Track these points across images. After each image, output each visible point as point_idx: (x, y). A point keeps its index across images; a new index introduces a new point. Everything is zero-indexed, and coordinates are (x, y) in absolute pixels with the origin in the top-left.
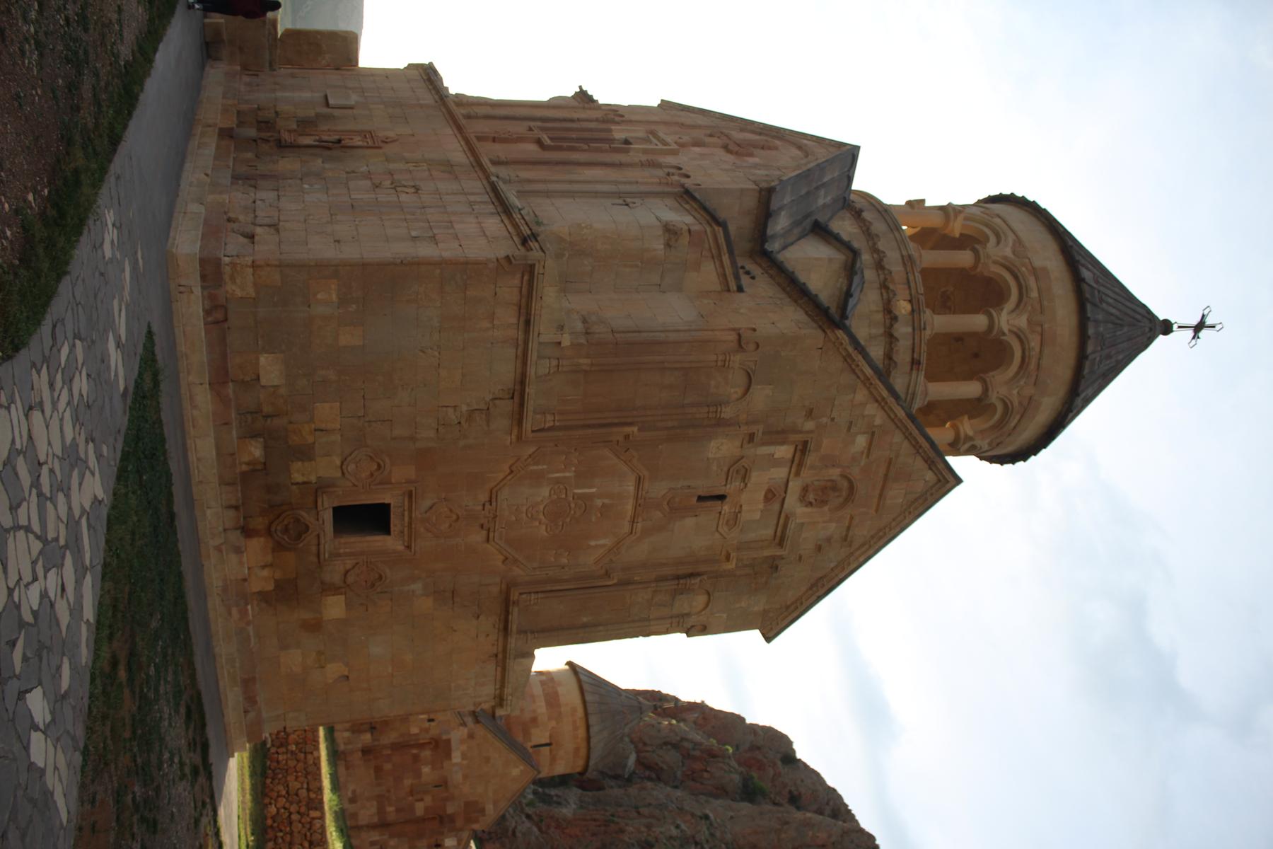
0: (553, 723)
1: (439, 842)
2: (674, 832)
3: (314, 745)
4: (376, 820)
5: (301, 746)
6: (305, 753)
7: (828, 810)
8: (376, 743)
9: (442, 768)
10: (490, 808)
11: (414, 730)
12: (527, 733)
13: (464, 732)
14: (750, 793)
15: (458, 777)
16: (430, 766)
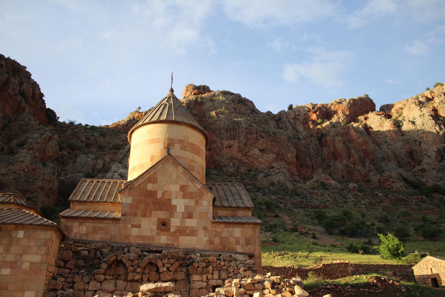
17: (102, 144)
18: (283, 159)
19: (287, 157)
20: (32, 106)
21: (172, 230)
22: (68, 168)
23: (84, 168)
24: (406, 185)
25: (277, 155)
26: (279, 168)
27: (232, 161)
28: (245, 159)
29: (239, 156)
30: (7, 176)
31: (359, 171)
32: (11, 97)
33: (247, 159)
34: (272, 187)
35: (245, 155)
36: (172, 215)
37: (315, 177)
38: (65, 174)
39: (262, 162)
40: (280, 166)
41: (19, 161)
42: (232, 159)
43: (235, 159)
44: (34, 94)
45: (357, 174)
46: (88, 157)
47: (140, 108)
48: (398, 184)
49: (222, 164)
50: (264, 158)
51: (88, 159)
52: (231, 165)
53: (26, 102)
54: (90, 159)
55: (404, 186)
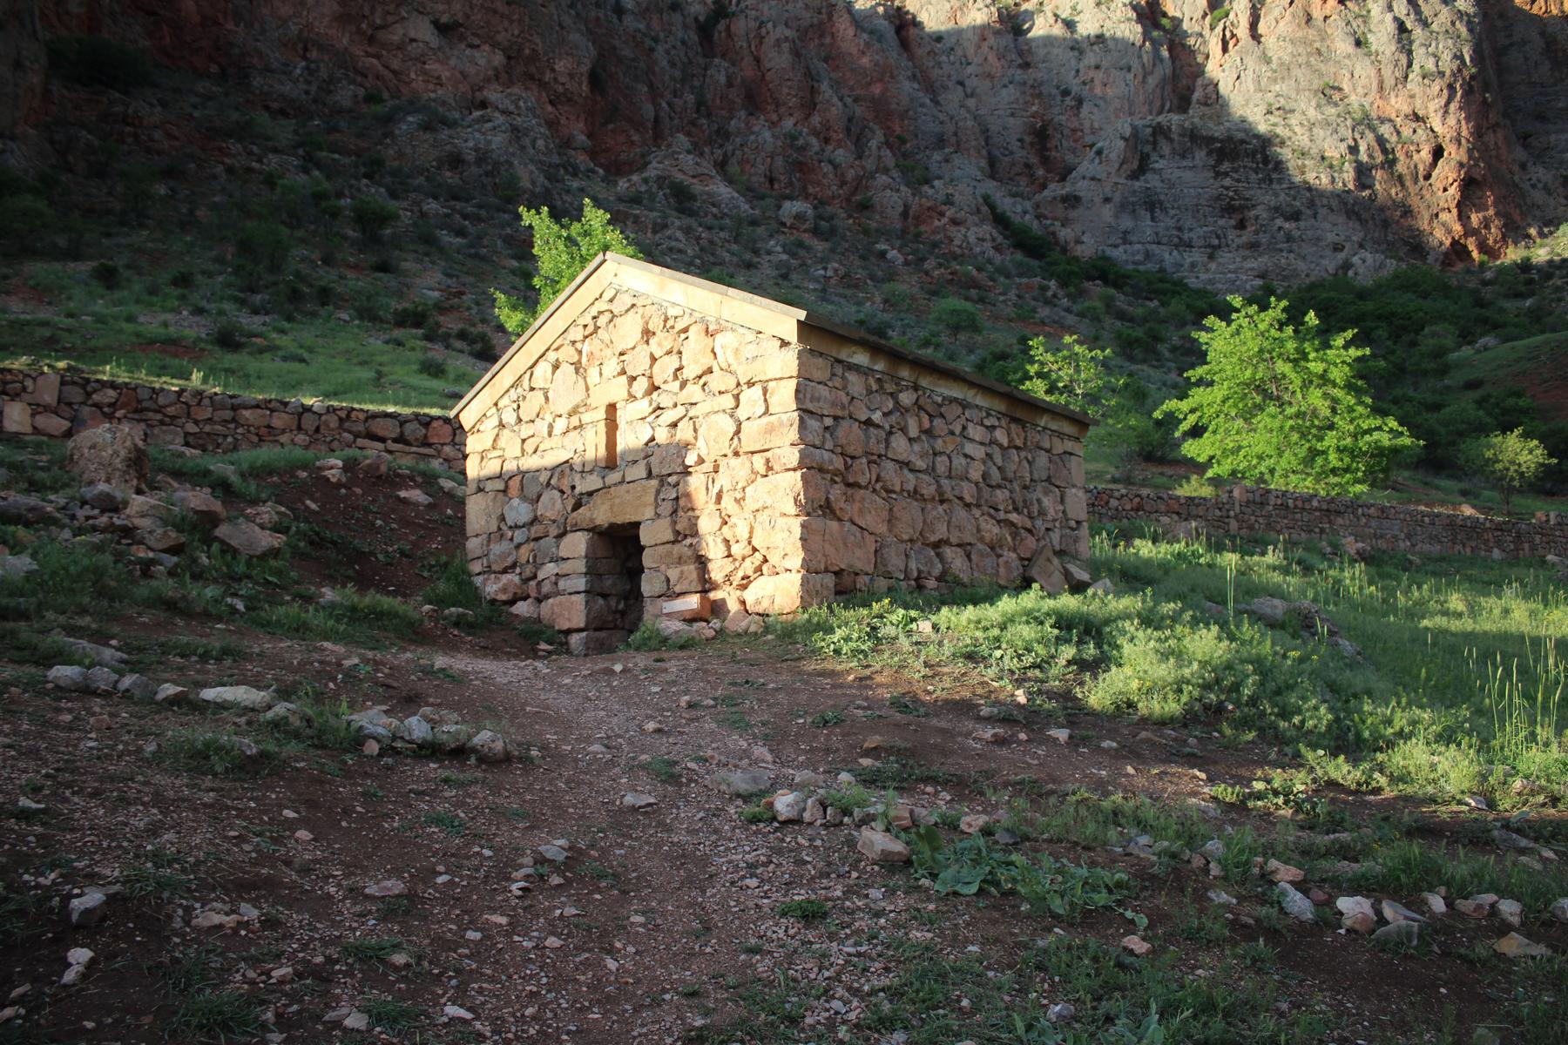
18: (532, 78)
19: (553, 70)
24: (1000, 239)
25: (509, 58)
26: (512, 108)
27: (304, 58)
28: (368, 55)
29: (344, 40)
31: (836, 167)
33: (377, 57)
34: (448, 174)
35: (371, 40)
37: (654, 164)
39: (439, 78)
40: (516, 103)
42: (306, 49)
43: (322, 48)
45: (825, 175)
48: (974, 229)
49: (255, 61)
50: (453, 62)
52: (298, 71)
55: (994, 240)
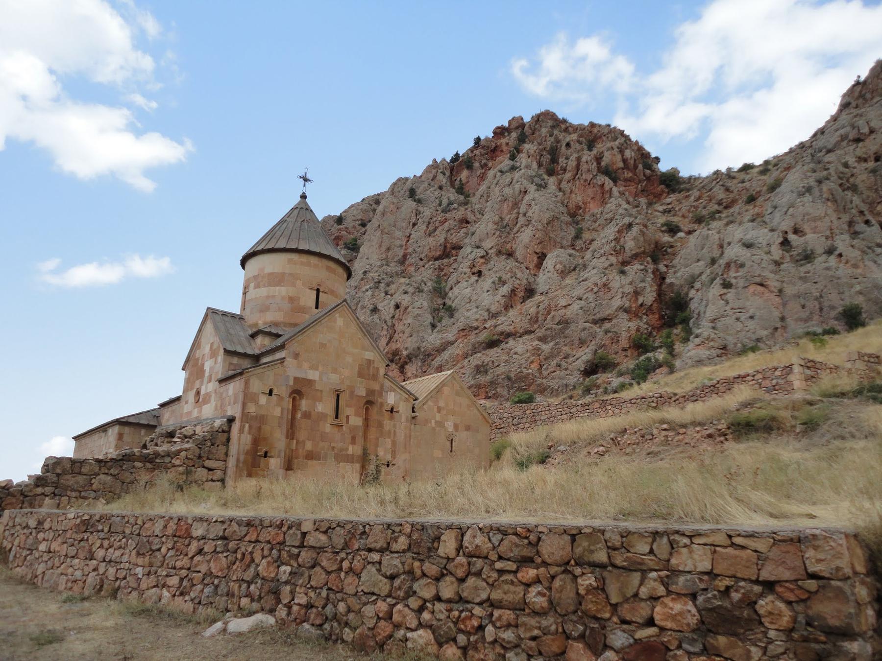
0: (298, 282)
1: (389, 408)
2: (369, 293)
3: (289, 528)
4: (358, 466)
5: (284, 554)
6: (302, 546)
7: (374, 206)
8: (283, 454)
9: (321, 391)
10: (369, 355)
11: (277, 412)
12: (302, 310)
13: (290, 361)
14: (354, 247)
15: (334, 378)
16: (317, 403)
17: (754, 191)
20: (630, 181)
21: (200, 400)
22: (677, 261)
23: (704, 251)
30: (570, 307)
32: (589, 184)
36: (202, 384)
38: (675, 273)
41: (583, 281)
44: (625, 161)
46: (709, 229)
47: (859, 77)
51: (710, 232)
53: (615, 180)
54: (713, 232)
